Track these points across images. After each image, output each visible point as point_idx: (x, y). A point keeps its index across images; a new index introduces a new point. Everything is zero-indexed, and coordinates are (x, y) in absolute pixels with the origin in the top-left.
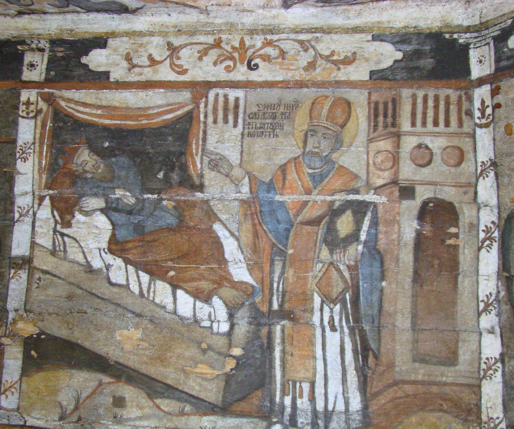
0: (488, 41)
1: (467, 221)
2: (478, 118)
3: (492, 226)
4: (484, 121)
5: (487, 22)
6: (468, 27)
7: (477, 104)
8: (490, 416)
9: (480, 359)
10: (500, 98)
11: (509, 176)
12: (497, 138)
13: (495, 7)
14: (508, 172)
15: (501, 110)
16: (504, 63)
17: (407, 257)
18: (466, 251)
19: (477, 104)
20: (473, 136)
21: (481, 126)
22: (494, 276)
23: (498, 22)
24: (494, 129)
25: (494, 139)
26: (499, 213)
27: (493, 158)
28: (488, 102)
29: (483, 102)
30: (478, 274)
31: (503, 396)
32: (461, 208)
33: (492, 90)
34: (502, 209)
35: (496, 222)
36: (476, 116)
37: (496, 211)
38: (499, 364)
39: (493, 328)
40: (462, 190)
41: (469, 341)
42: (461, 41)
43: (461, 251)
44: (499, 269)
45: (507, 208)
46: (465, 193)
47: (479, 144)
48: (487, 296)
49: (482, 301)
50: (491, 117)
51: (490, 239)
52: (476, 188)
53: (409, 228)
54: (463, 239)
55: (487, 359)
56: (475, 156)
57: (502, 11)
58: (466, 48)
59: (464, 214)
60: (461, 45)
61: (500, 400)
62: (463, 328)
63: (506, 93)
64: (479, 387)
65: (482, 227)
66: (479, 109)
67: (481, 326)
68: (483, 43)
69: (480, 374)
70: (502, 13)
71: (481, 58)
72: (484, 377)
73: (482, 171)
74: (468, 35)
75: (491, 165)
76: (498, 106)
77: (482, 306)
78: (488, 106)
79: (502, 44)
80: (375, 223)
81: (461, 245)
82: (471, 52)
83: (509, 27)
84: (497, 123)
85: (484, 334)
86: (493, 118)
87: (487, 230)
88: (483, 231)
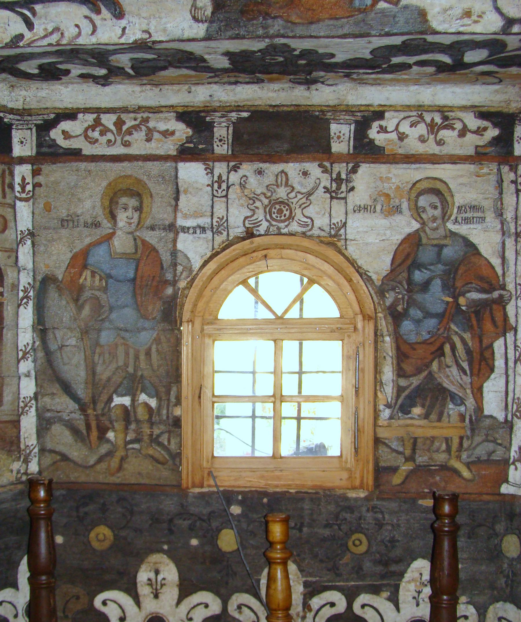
0: (30, 126)
1: (11, 281)
2: (18, 192)
3: (28, 286)
4: (24, 195)
5: (31, 109)
6: (12, 109)
8: (27, 444)
9: (19, 398)
10: (40, 179)
11: (45, 245)
12: (36, 212)
13: (38, 99)
14: (45, 242)
15: (42, 189)
16: (44, 150)
18: (9, 307)
19: (18, 180)
20: (14, 207)
21: (21, 200)
22: (30, 329)
23: (40, 113)
24: (33, 204)
25: (33, 213)
26: (34, 276)
27: (31, 228)
28: (29, 179)
29: (23, 179)
30: (17, 328)
31: (37, 427)
32: (6, 270)
33: (33, 170)
34: (37, 273)
35: (32, 283)
36: (16, 190)
37: (31, 274)
38: (33, 402)
39: (29, 372)
40: (7, 254)
41: (11, 385)
42: (6, 120)
43: (5, 307)
44: (34, 323)
45: (41, 272)
46: (9, 257)
47: (18, 215)
48: (25, 346)
49: (21, 350)
50: (31, 193)
51: (27, 297)
52: (17, 253)
54: (7, 297)
55: (24, 398)
56: (16, 225)
57: (45, 104)
58: (9, 127)
59: (8, 275)
60: (5, 123)
61: (35, 430)
62: (7, 374)
63: (47, 175)
64: (19, 421)
65: (21, 288)
66: (19, 184)
67: (20, 372)
68: (25, 127)
69: (19, 411)
70: (45, 106)
71: (23, 140)
72: (22, 413)
73: (21, 239)
74: (11, 116)
75: (28, 235)
76: (39, 185)
77: (21, 354)
78: (28, 183)
79: (44, 133)
81: (5, 302)
82: (14, 132)
83: (52, 119)
84: (36, 199)
85: (22, 378)
86: (33, 194)
87: (25, 291)
88: (22, 290)
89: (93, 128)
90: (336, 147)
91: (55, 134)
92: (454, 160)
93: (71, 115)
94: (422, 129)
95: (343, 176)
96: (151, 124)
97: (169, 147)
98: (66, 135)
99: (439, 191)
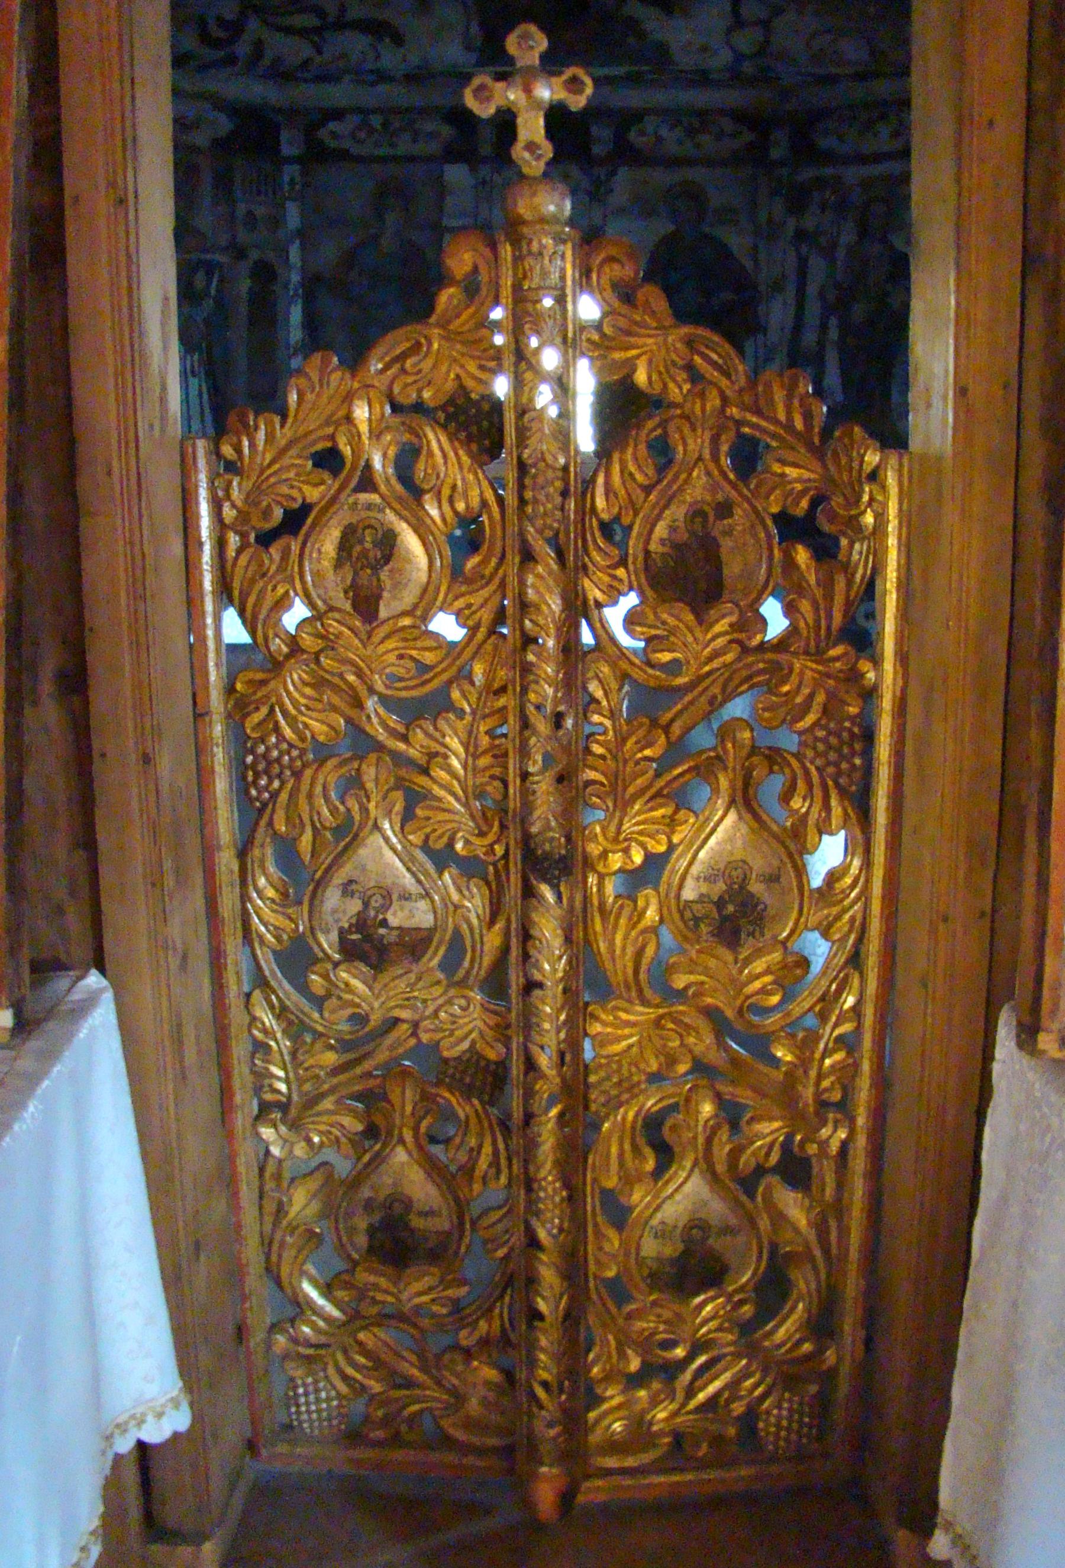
7: (286, 179)
17: (244, 309)
19: (286, 179)
20: (283, 206)
28: (298, 179)
29: (292, 180)
53: (245, 285)
58: (277, 129)
65: (292, 286)
77: (292, 350)
80: (221, 281)
89: (359, 128)
90: (597, 150)
91: (323, 133)
92: (710, 163)
93: (338, 114)
94: (679, 132)
95: (603, 178)
96: (417, 126)
97: (434, 148)
98: (334, 135)
99: (694, 195)
